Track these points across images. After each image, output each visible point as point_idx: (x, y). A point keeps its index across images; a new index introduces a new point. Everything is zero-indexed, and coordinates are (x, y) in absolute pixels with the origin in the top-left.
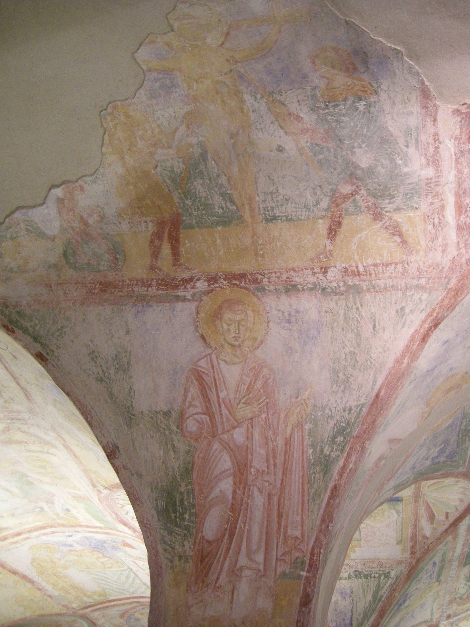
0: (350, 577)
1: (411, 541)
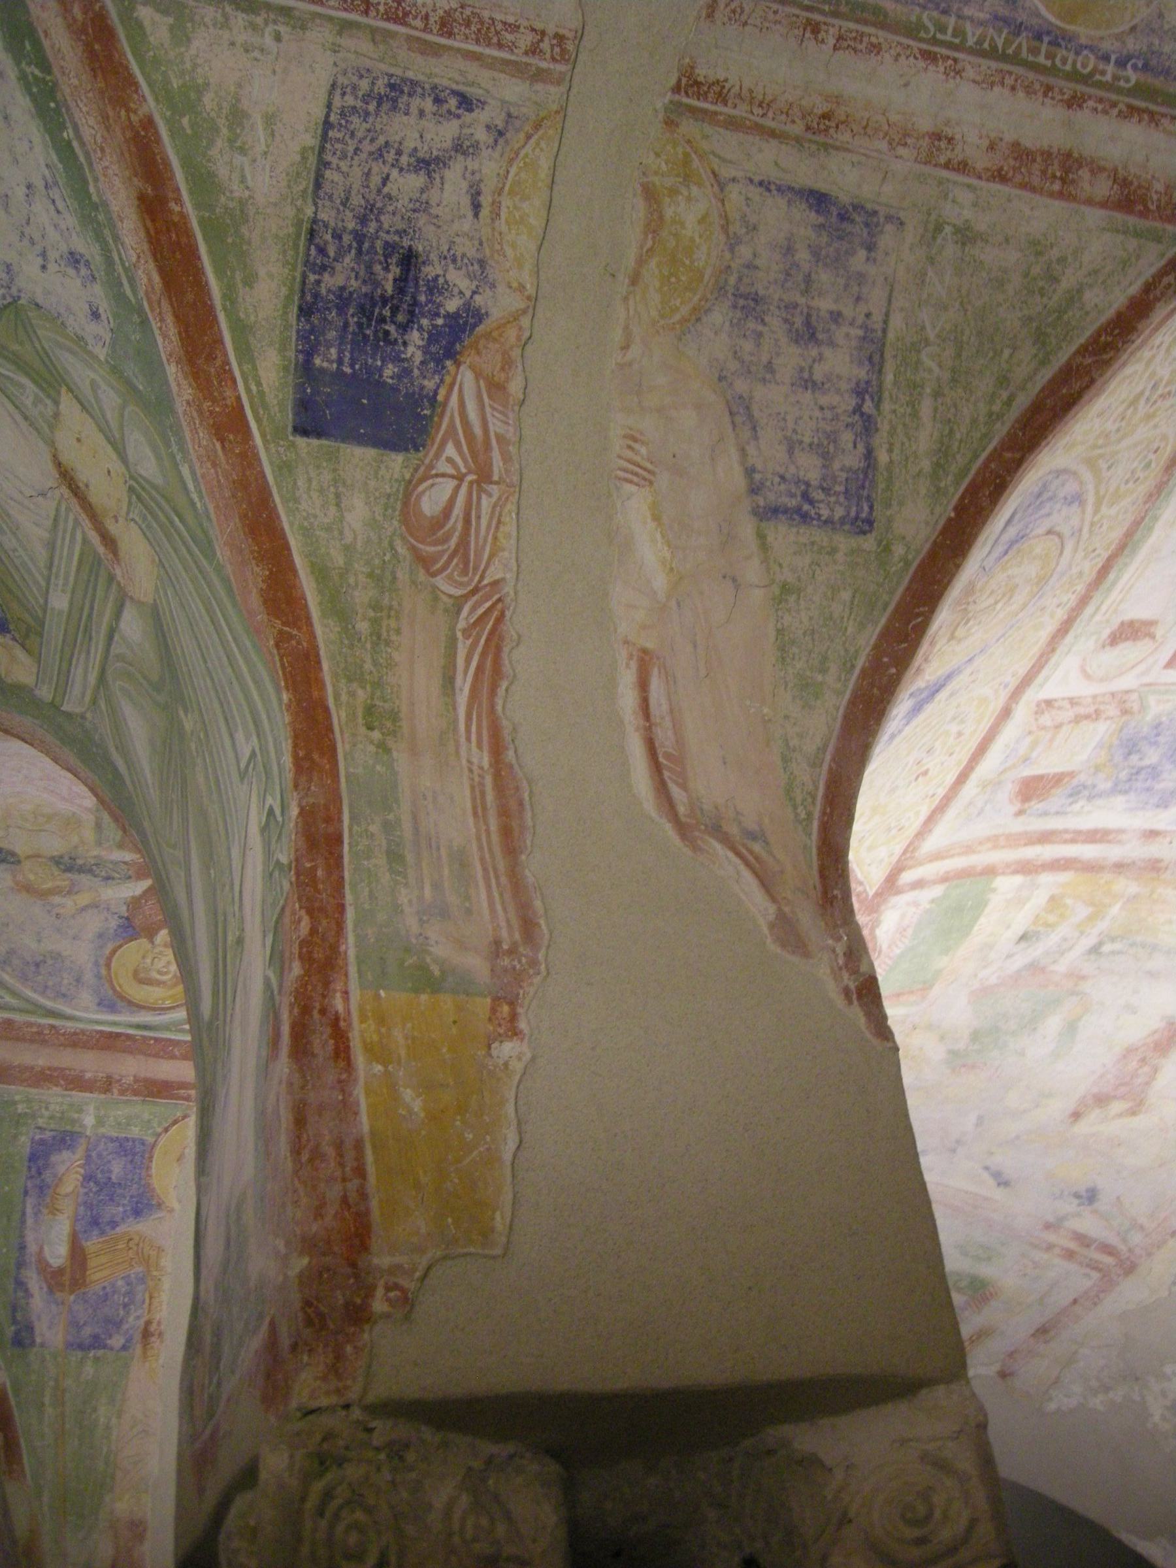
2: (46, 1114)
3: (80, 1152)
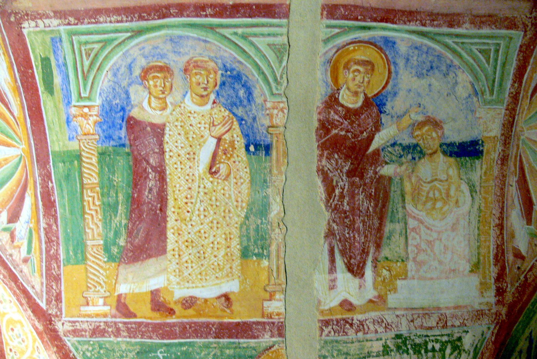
1: (495, 265)
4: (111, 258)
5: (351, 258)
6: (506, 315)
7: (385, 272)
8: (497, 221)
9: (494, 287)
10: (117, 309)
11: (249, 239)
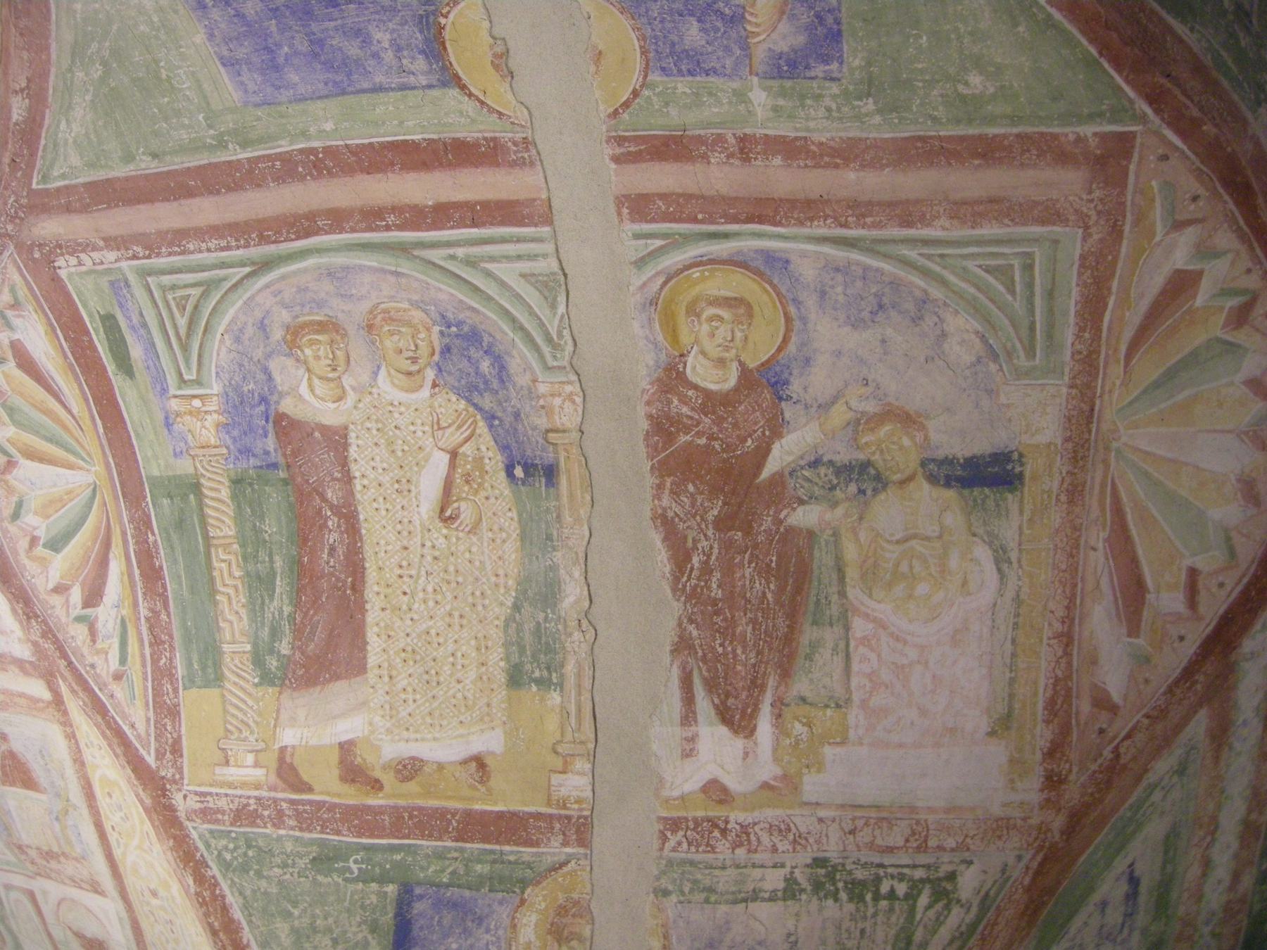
0: (791, 891)
2: (827, 101)
3: (760, 54)
4: (266, 678)
5: (728, 695)
6: (1062, 833)
7: (798, 728)
8: (1058, 626)
9: (1039, 771)
10: (279, 774)
11: (522, 650)
